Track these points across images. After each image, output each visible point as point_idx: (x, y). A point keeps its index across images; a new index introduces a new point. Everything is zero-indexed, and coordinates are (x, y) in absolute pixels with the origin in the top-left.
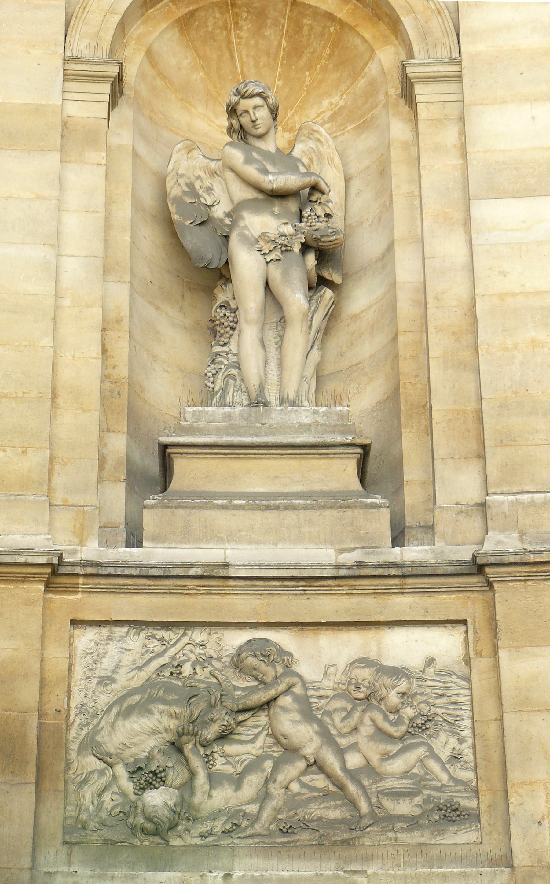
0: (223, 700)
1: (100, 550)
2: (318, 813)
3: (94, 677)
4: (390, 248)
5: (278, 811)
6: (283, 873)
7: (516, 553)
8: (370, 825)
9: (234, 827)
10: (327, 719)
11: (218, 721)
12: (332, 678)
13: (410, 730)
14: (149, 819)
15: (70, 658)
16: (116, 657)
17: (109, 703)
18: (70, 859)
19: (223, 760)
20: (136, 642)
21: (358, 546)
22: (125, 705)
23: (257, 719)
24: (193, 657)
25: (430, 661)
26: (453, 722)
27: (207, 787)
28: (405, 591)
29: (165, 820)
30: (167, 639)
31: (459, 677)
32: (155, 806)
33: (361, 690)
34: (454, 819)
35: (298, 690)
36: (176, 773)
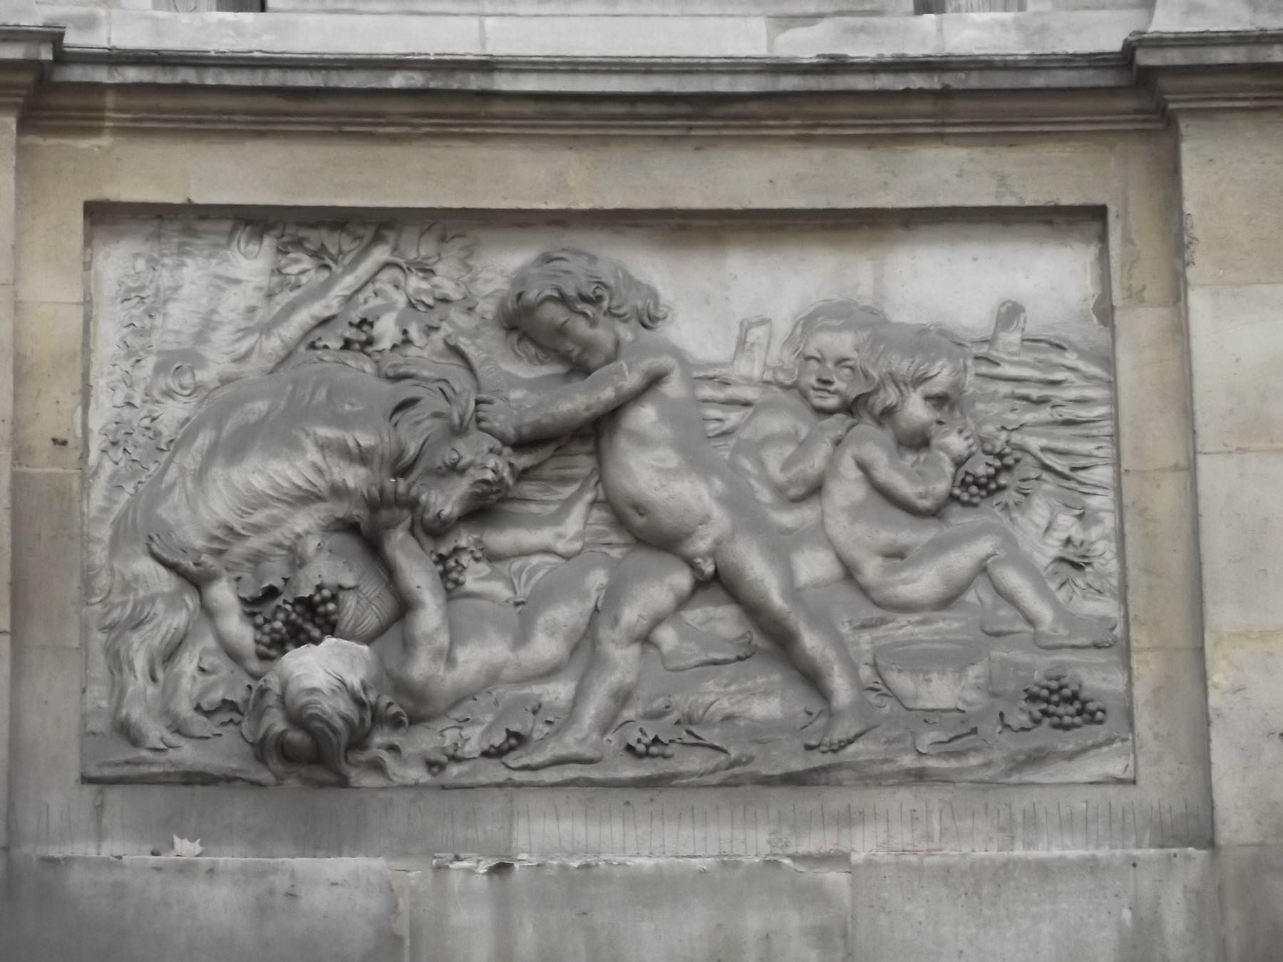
0: (481, 414)
1: (157, 19)
2: (725, 705)
3: (148, 352)
5: (623, 697)
6: (638, 861)
7: (1238, 39)
8: (858, 736)
9: (513, 741)
10: (747, 464)
11: (471, 471)
12: (758, 354)
13: (957, 492)
14: (299, 719)
15: (87, 303)
16: (204, 301)
17: (187, 419)
18: (99, 821)
19: (484, 568)
21: (826, 8)
22: (229, 426)
23: (569, 460)
24: (401, 300)
25: (1010, 313)
26: (1067, 471)
27: (443, 639)
28: (948, 130)
29: (338, 723)
30: (334, 251)
31: (1082, 355)
32: (313, 691)
33: (832, 388)
34: (1067, 720)
35: (673, 388)
36: (363, 602)
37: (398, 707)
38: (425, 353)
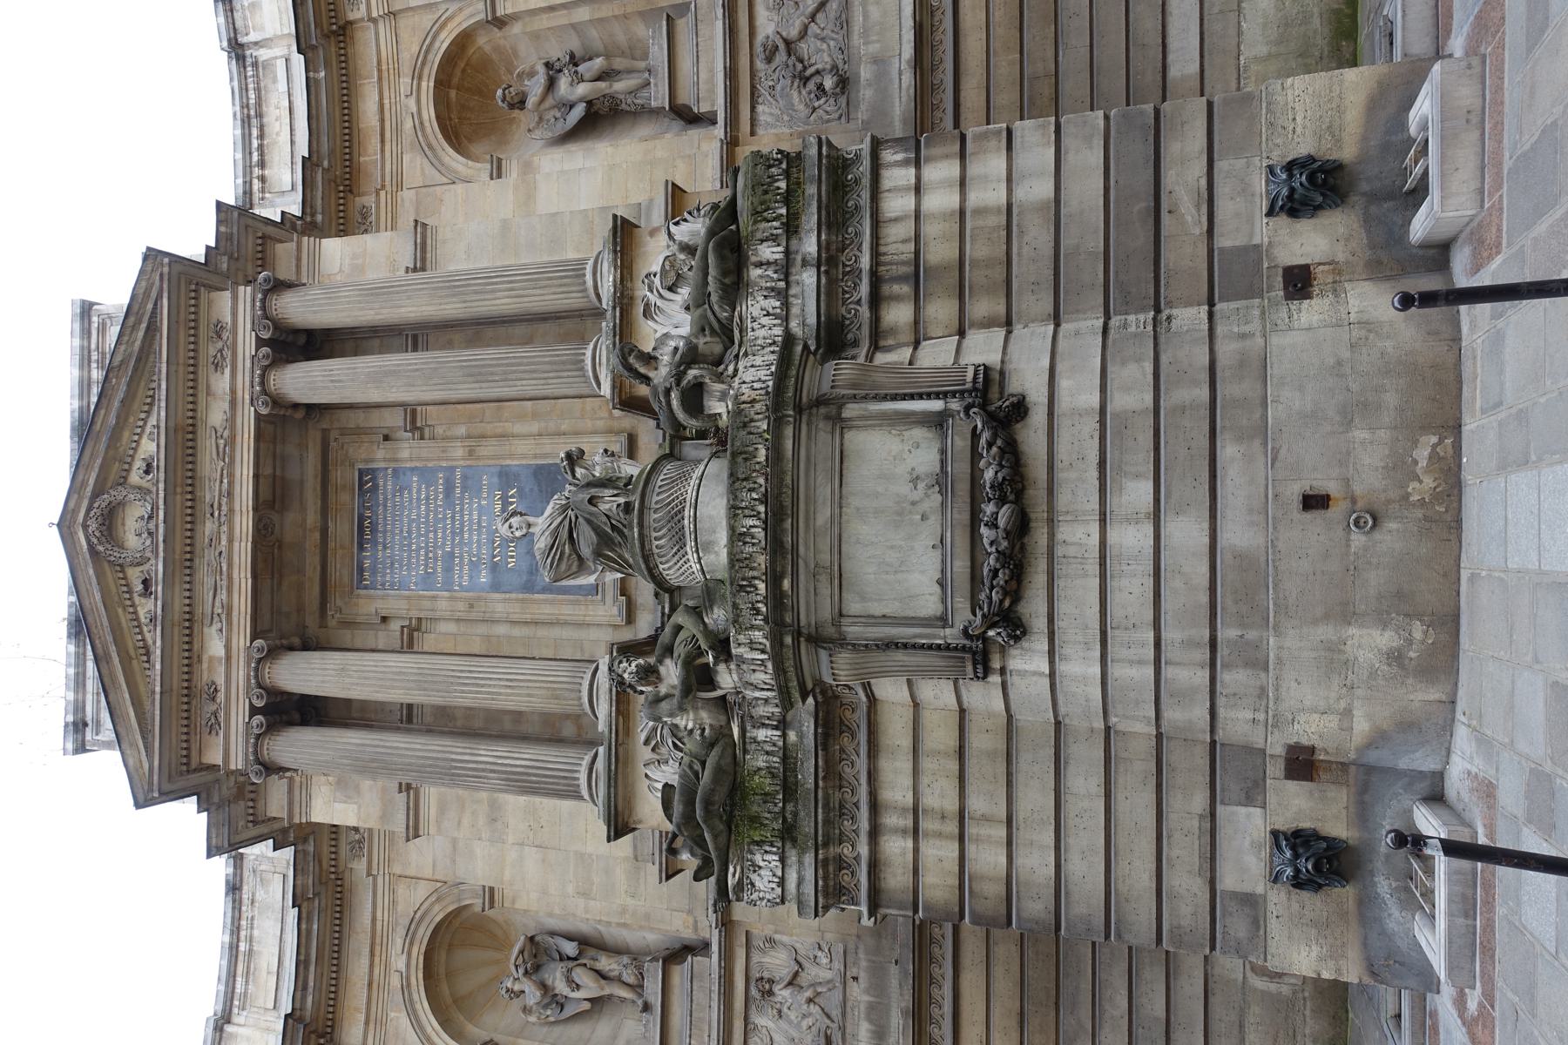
4: (573, 26)
20: (760, 108)
37: (835, 67)
38: (775, 77)
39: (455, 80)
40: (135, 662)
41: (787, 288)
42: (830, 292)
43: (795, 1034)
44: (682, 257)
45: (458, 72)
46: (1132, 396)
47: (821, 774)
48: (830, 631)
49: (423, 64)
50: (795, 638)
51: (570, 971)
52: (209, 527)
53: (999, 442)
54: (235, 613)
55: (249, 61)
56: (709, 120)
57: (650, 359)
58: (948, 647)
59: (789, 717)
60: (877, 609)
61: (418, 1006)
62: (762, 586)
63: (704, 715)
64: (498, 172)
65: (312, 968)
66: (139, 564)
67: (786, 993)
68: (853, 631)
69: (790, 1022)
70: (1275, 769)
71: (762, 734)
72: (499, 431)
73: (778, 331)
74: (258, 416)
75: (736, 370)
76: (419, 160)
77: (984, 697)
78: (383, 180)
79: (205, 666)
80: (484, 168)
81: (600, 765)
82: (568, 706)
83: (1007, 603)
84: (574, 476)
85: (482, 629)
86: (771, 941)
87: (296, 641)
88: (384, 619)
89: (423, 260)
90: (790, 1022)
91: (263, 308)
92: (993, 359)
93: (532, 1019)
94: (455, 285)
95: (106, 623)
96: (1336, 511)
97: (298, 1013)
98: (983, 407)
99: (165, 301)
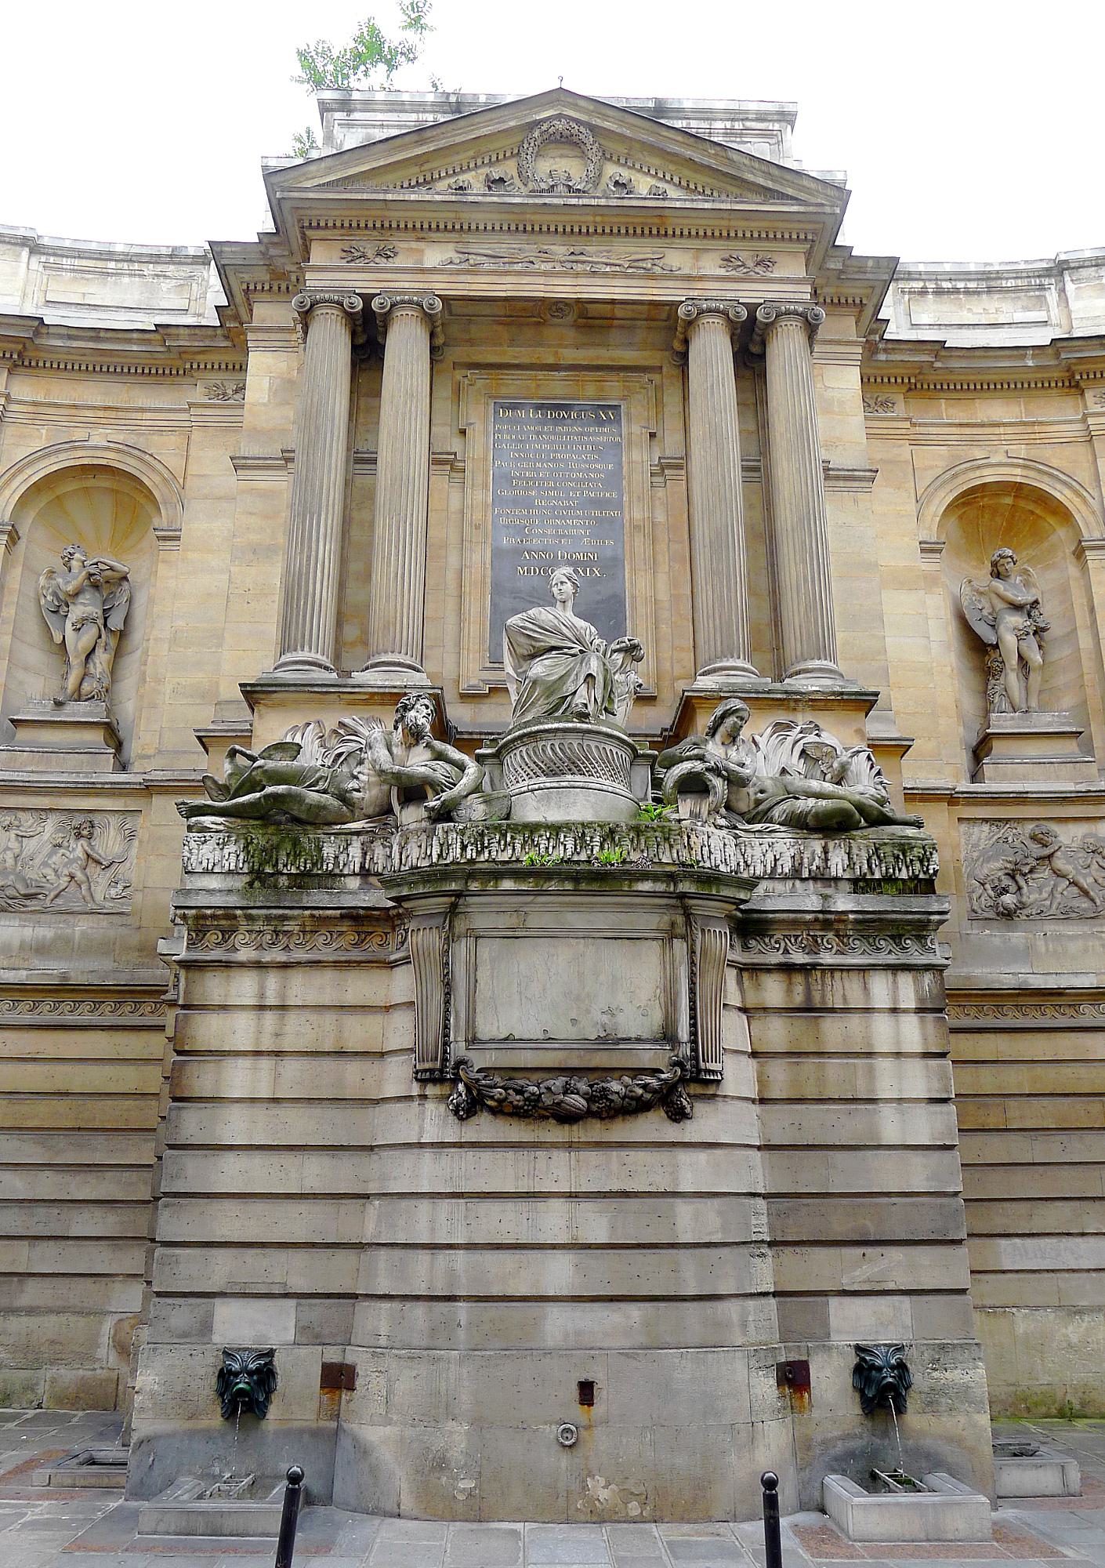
20: (986, 827)
37: (1022, 906)
38: (1017, 843)
39: (1022, 504)
40: (416, 169)
41: (803, 880)
42: (795, 922)
43: (37, 861)
44: (835, 765)
45: (1031, 507)
46: (689, 1222)
47: (315, 912)
48: (460, 926)
49: (1040, 471)
50: (450, 891)
51: (94, 621)
52: (560, 250)
53: (648, 1096)
54: (469, 278)
55: (1046, 281)
56: (975, 777)
57: (733, 737)
58: (446, 1044)
59: (373, 880)
60: (483, 975)
61: (53, 459)
62: (505, 856)
63: (375, 791)
64: (929, 549)
65: (91, 345)
66: (520, 174)
67: (79, 853)
68: (461, 950)
69: (50, 855)
70: (333, 1355)
71: (355, 851)
72: (660, 558)
73: (759, 871)
74: (675, 305)
75: (721, 827)
76: (941, 465)
77: (397, 1077)
78: (920, 425)
79: (414, 245)
80: (931, 534)
81: (319, 676)
82: (376, 639)
83: (490, 1103)
84: (615, 651)
85: (453, 538)
86: (132, 836)
87: (440, 341)
88: (463, 432)
89: (837, 478)
90: (50, 855)
91: (788, 313)
92: (729, 1087)
93: (42, 581)
94: (811, 518)
95: (458, 139)
96: (579, 1412)
97: (44, 330)
98: (682, 1080)
99: (795, 209)
